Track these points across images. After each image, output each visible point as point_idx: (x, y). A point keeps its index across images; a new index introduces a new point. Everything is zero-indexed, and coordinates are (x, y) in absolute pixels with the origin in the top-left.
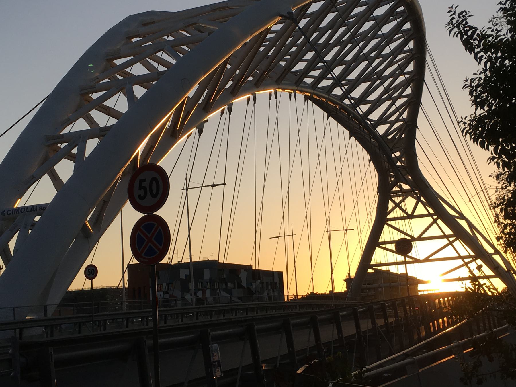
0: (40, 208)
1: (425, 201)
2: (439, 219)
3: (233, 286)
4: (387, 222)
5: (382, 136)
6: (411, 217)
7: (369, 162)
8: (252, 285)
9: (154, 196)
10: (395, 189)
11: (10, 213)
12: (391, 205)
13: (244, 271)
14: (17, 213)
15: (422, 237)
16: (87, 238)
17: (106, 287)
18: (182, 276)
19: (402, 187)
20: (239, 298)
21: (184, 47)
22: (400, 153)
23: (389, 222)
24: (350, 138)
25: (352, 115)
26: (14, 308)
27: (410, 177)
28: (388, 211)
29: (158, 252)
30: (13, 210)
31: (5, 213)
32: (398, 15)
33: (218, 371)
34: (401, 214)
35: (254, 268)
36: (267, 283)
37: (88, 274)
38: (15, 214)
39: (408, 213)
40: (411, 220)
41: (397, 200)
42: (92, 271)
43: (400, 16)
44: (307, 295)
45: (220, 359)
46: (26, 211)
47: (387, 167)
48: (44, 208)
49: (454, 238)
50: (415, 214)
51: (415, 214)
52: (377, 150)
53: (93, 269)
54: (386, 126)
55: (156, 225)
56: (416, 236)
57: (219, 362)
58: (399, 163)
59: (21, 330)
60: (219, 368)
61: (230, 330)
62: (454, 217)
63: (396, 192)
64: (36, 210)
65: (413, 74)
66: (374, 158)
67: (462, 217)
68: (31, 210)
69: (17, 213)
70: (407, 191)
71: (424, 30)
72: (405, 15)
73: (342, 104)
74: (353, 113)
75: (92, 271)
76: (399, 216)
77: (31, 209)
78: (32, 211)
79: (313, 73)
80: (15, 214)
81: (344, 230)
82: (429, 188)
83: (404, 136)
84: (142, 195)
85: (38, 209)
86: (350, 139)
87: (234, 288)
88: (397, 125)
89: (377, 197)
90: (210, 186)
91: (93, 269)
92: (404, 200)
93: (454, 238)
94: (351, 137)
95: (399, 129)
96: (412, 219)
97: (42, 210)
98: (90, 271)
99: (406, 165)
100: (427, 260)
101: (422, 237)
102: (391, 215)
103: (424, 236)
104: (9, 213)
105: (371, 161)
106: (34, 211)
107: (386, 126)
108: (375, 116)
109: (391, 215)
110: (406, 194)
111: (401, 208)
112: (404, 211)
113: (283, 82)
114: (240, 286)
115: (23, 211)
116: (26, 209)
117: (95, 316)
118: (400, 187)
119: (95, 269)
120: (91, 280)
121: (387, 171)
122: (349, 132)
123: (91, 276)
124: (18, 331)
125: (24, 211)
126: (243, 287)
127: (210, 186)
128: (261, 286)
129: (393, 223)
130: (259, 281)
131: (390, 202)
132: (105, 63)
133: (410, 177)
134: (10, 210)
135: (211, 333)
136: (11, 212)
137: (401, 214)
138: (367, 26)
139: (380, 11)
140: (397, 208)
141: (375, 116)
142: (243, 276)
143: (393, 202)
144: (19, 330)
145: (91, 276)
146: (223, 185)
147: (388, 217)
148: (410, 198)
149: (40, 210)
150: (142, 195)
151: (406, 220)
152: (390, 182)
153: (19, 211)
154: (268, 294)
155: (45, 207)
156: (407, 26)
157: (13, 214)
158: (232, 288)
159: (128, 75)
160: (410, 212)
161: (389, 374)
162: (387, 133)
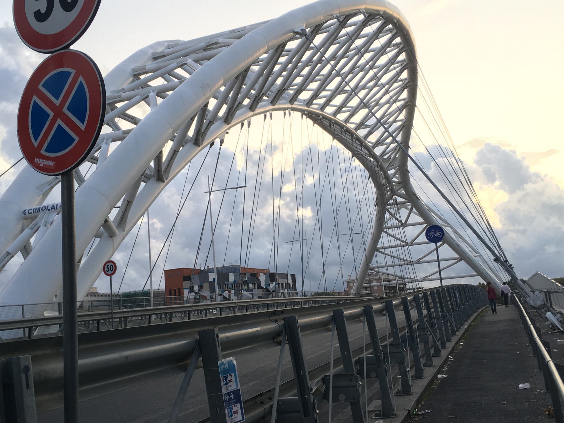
3: (254, 287)
6: (404, 225)
7: (369, 178)
8: (270, 286)
9: (68, 7)
10: (391, 201)
11: (31, 212)
12: (387, 216)
13: (263, 274)
14: (38, 212)
16: (112, 237)
17: (148, 290)
18: (211, 279)
20: (259, 297)
22: (395, 171)
26: (23, 306)
27: (403, 191)
28: (385, 220)
29: (77, 139)
30: (34, 209)
31: (27, 212)
32: (394, 46)
33: (236, 412)
34: (396, 223)
36: (282, 284)
37: (107, 271)
38: (36, 212)
39: (403, 222)
40: (405, 228)
42: (110, 268)
43: (396, 47)
45: (239, 387)
46: (47, 210)
52: (376, 169)
53: (112, 265)
54: (383, 147)
55: (73, 72)
56: (409, 242)
57: (236, 393)
58: (394, 179)
59: (30, 328)
60: (238, 405)
61: (258, 329)
63: (393, 204)
64: (57, 209)
65: (406, 101)
66: (373, 176)
68: (52, 208)
69: (38, 212)
70: (402, 203)
72: (402, 46)
74: (356, 134)
75: (110, 268)
76: (395, 224)
77: (52, 207)
78: (53, 210)
79: (323, 93)
80: (36, 212)
82: (419, 199)
83: (399, 156)
84: (43, 11)
86: (352, 159)
87: (255, 288)
88: (393, 146)
90: (231, 188)
91: (112, 265)
92: (398, 210)
94: (353, 157)
95: (394, 149)
96: (406, 227)
98: (108, 267)
99: (400, 181)
101: (415, 241)
102: (389, 224)
103: (416, 241)
104: (30, 212)
106: (55, 209)
107: (383, 147)
108: (373, 138)
109: (389, 224)
111: (397, 219)
113: (295, 103)
114: (260, 287)
115: (44, 209)
116: (46, 207)
117: (115, 313)
119: (113, 265)
120: (109, 277)
121: (385, 186)
123: (110, 272)
124: (27, 330)
125: (45, 210)
126: (262, 288)
127: (231, 188)
128: (277, 286)
129: (390, 231)
130: (274, 283)
132: (132, 79)
134: (31, 209)
135: (221, 336)
136: (32, 211)
137: (396, 223)
138: (367, 56)
139: (377, 44)
141: (373, 138)
142: (262, 278)
143: (390, 212)
144: (28, 329)
145: (110, 272)
146: (244, 188)
150: (43, 11)
151: (401, 228)
153: (40, 210)
154: (283, 293)
156: (402, 56)
157: (34, 213)
158: (253, 289)
160: (403, 222)
161: (444, 376)
162: (384, 153)
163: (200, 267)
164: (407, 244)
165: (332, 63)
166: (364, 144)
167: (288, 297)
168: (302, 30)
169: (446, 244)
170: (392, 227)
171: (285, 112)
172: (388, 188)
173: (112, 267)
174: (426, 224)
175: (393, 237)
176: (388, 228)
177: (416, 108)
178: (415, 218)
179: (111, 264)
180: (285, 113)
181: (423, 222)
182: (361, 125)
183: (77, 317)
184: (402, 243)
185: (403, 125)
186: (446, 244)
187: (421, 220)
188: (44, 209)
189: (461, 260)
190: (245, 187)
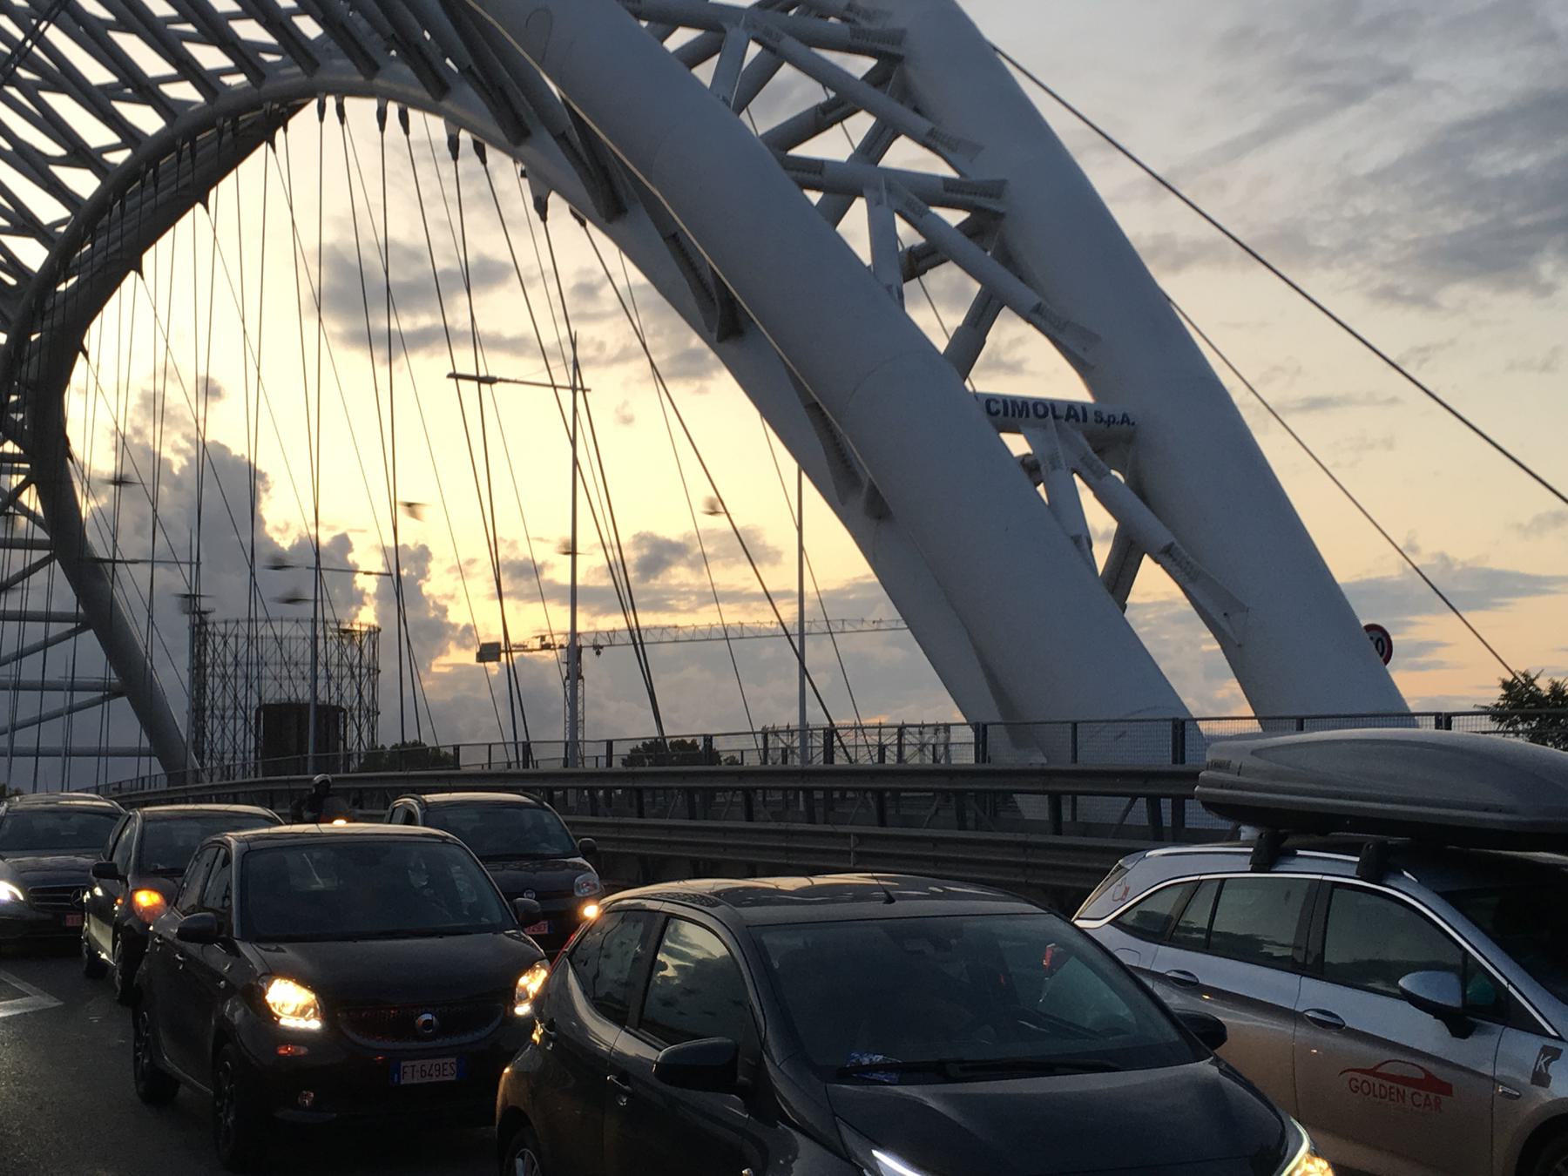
0: (1096, 413)
11: (998, 412)
14: (1020, 415)
16: (880, 518)
38: (1013, 415)
48: (1112, 419)
64: (1085, 420)
69: (1020, 415)
70: (13, 458)
80: (1013, 415)
85: (1091, 416)
93: (72, 626)
97: (1103, 423)
104: (994, 407)
106: (1078, 420)
108: (48, 210)
115: (1041, 410)
119: (1384, 639)
134: (997, 402)
136: (1001, 406)
141: (48, 210)
149: (1096, 421)
155: (1113, 416)
167: (344, 772)
169: (92, 631)
171: (341, 101)
173: (1380, 644)
179: (1380, 635)
180: (382, 117)
181: (44, 541)
183: (785, 766)
186: (92, 631)
187: (41, 535)
188: (1041, 410)
189: (112, 693)
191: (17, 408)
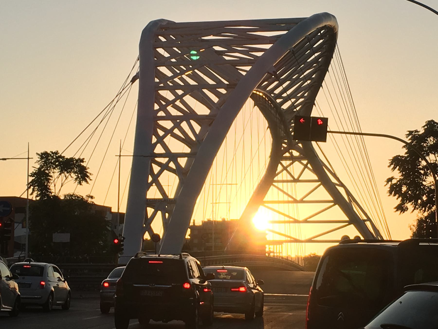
1: (312, 168)
2: (322, 186)
4: (274, 183)
5: (279, 104)
7: (268, 128)
10: (287, 154)
12: (280, 168)
15: (304, 200)
19: (293, 154)
21: (182, 67)
23: (275, 184)
24: (254, 106)
25: (268, 98)
27: (300, 145)
28: (277, 173)
35: (113, 211)
40: (296, 184)
41: (285, 163)
44: (269, 253)
47: (282, 135)
49: (333, 204)
50: (300, 179)
51: (300, 179)
56: (298, 199)
62: (335, 184)
67: (342, 185)
71: (337, 38)
73: (265, 92)
81: (227, 184)
82: (317, 157)
89: (268, 160)
100: (306, 221)
101: (304, 200)
105: (269, 129)
110: (293, 159)
112: (292, 177)
118: (291, 154)
122: (253, 102)
131: (279, 165)
133: (300, 145)
137: (290, 178)
140: (285, 171)
147: (276, 179)
148: (297, 163)
151: (293, 183)
152: (282, 149)
159: (165, 100)
160: (296, 177)
163: (33, 197)
164: (295, 201)
165: (293, 100)
166: (274, 104)
168: (274, 72)
170: (283, 181)
172: (286, 141)
174: (320, 183)
175: (284, 193)
176: (278, 181)
177: (327, 72)
178: (309, 175)
182: (279, 96)
184: (290, 199)
185: (312, 85)
187: (315, 177)
189: (350, 223)
190: (236, 184)
191: (298, 143)
